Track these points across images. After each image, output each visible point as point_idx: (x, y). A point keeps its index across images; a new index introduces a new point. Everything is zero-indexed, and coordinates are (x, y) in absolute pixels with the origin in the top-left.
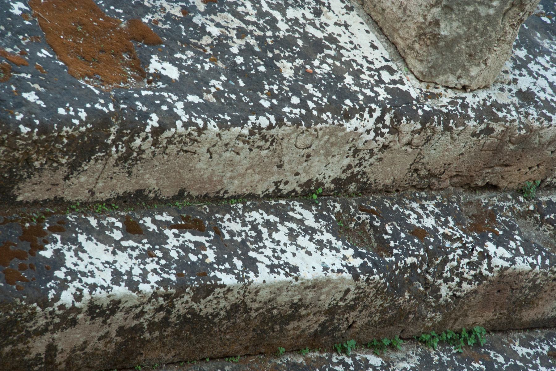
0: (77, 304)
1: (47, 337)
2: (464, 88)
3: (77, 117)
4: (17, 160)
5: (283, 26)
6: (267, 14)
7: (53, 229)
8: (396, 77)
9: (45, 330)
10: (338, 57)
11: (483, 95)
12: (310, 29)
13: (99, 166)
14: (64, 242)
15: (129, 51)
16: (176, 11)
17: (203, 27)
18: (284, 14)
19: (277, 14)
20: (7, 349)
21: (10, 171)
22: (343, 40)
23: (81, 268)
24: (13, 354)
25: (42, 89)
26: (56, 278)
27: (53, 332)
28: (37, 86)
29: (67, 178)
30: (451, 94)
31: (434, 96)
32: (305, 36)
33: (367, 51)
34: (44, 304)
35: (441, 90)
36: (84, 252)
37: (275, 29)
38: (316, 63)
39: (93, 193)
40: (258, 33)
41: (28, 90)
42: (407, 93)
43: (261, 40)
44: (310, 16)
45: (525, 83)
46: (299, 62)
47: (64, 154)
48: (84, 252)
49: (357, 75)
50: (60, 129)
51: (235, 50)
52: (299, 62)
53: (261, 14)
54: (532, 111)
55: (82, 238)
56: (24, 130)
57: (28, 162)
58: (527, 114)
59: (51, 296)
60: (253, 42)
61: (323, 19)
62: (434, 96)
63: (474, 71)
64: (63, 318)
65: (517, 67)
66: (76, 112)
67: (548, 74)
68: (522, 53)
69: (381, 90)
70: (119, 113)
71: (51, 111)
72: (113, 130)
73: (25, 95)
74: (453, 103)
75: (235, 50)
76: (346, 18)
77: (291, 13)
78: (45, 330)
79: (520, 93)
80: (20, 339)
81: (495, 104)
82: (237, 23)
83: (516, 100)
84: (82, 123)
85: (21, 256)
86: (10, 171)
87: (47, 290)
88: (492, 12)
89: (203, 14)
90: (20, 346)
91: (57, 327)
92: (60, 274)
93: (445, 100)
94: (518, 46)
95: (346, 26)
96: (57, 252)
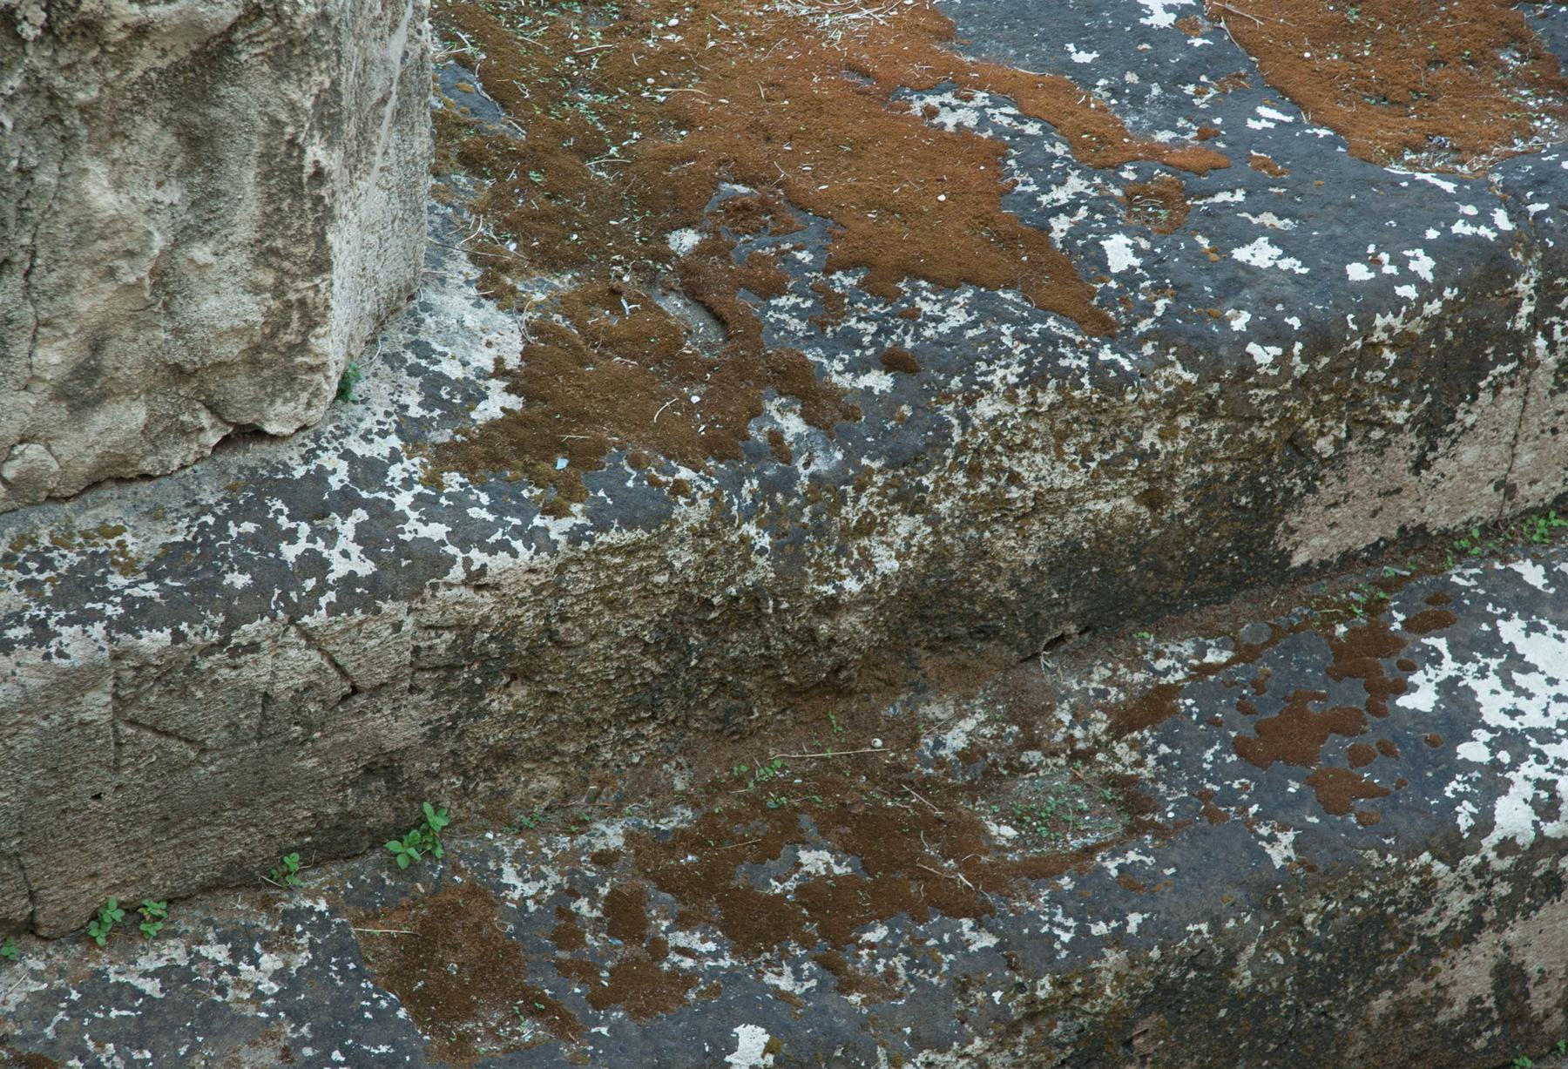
0: (1551, 829)
1: (1486, 945)
3: (1409, 277)
4: (1264, 448)
7: (1419, 625)
9: (1477, 924)
13: (1509, 404)
14: (1461, 657)
15: (1516, 38)
20: (1381, 1004)
21: (1253, 486)
23: (1533, 718)
24: (1400, 1015)
25: (1286, 224)
26: (1468, 766)
27: (1500, 926)
28: (1268, 219)
29: (1420, 464)
34: (1453, 848)
36: (1528, 668)
39: (1507, 488)
41: (1246, 238)
47: (1397, 395)
48: (1528, 668)
50: (1366, 327)
55: (1511, 630)
56: (1263, 355)
57: (1297, 445)
59: (1464, 822)
64: (1518, 877)
66: (1402, 263)
70: (1529, 233)
71: (1326, 279)
72: (1524, 286)
73: (1240, 254)
78: (1477, 924)
80: (1412, 968)
84: (1427, 291)
85: (1346, 724)
86: (1253, 486)
87: (1450, 806)
90: (1416, 987)
91: (1509, 908)
92: (1474, 750)
96: (1448, 688)
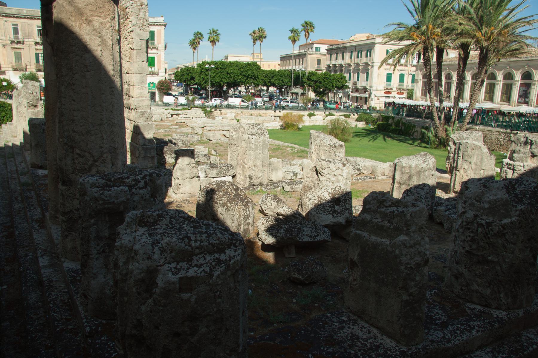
2: (417, 344)
5: (368, 345)
6: (364, 343)
8: (400, 348)
10: (384, 348)
11: (422, 344)
12: (375, 343)
16: (343, 351)
17: (350, 352)
18: (367, 342)
19: (366, 343)
22: (384, 343)
30: (414, 347)
31: (410, 349)
32: (374, 345)
33: (390, 344)
35: (412, 347)
37: (367, 346)
38: (380, 351)
40: (363, 349)
42: (404, 351)
43: (365, 350)
44: (374, 340)
45: (430, 338)
46: (375, 352)
49: (390, 350)
51: (359, 355)
52: (375, 352)
53: (362, 344)
54: (435, 344)
58: (434, 345)
60: (363, 351)
61: (377, 340)
62: (410, 349)
63: (417, 340)
65: (427, 335)
67: (435, 334)
68: (426, 331)
69: (397, 352)
74: (416, 349)
75: (359, 355)
76: (382, 338)
77: (369, 341)
79: (430, 341)
81: (425, 346)
82: (358, 348)
83: (430, 343)
88: (415, 324)
89: (349, 349)
93: (414, 349)
94: (425, 330)
95: (383, 339)
